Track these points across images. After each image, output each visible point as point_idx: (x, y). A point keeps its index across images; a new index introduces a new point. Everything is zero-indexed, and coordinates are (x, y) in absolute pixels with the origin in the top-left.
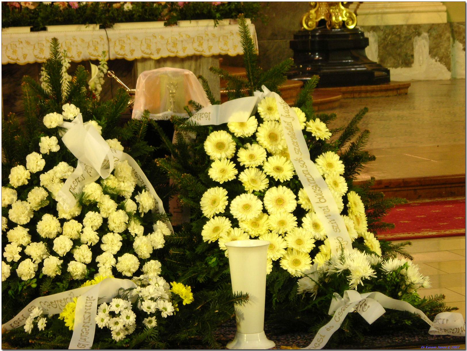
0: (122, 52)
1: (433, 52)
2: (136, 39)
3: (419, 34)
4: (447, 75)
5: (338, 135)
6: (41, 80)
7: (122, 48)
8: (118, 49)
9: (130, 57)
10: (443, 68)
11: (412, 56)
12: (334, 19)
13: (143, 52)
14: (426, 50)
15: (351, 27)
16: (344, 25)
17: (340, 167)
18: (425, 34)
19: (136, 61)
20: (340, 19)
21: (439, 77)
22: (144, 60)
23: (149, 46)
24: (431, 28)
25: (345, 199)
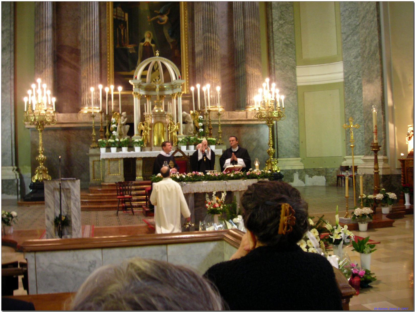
0: (230, 189)
1: (300, 178)
2: (234, 185)
3: (295, 172)
4: (304, 185)
5: (316, 223)
6: (206, 197)
7: (230, 188)
8: (229, 188)
9: (232, 190)
10: (302, 182)
11: (293, 179)
12: (273, 169)
13: (236, 189)
14: (298, 177)
15: (278, 172)
16: (276, 171)
17: (317, 233)
18: (297, 172)
19: (234, 191)
20: (275, 169)
21: (302, 185)
22: (236, 191)
23: (238, 187)
24: (299, 170)
25: (319, 242)
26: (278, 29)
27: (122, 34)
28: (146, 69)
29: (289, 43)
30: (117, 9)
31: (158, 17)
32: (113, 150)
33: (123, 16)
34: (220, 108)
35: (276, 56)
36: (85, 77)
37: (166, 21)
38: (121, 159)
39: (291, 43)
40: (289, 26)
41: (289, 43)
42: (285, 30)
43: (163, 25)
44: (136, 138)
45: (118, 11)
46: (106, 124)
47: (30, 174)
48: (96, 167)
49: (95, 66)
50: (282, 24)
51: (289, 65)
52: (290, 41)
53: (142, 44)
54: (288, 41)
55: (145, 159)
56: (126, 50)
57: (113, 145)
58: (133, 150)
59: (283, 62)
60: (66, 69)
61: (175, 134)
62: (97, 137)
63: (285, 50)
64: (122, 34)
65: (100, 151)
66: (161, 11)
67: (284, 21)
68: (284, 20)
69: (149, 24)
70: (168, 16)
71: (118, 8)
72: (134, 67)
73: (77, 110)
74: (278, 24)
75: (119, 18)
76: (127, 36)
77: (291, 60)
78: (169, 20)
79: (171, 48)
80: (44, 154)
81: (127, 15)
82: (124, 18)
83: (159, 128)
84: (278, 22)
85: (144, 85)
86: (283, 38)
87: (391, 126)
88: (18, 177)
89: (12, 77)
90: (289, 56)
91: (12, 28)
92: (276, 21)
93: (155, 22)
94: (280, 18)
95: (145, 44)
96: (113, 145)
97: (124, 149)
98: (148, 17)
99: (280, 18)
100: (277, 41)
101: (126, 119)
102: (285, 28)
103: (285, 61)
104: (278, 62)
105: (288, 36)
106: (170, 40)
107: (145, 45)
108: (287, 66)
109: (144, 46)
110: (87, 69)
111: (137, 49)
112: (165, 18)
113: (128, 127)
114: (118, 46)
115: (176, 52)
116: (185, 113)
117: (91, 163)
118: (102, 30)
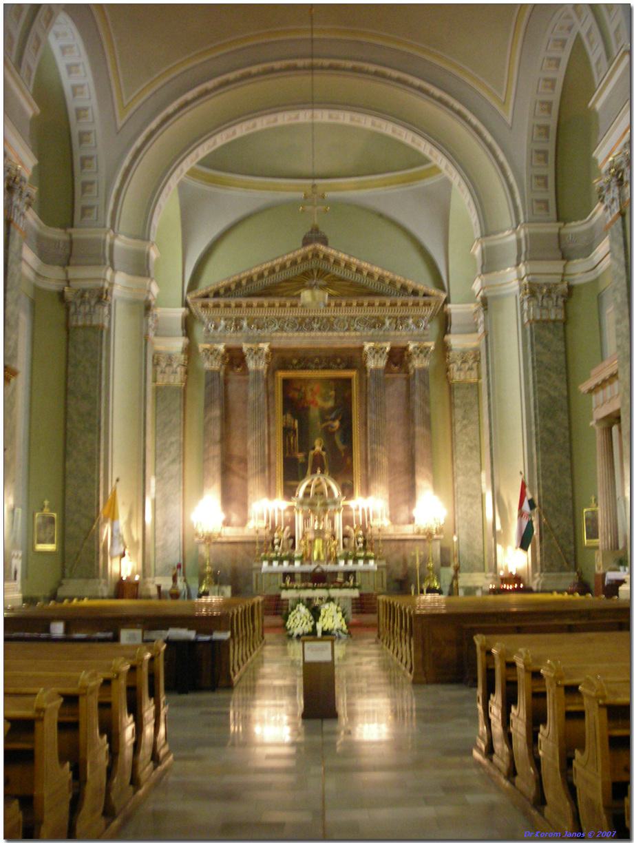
28: (309, 487)
31: (329, 423)
32: (275, 563)
34: (386, 522)
35: (458, 462)
37: (337, 427)
44: (297, 554)
46: (270, 538)
47: (197, 586)
48: (259, 580)
56: (296, 460)
57: (276, 559)
58: (294, 564)
59: (466, 466)
60: (235, 480)
61: (332, 549)
62: (261, 551)
63: (469, 453)
65: (262, 564)
66: (333, 416)
70: (340, 421)
72: (304, 476)
73: (244, 523)
76: (297, 446)
78: (341, 426)
79: (343, 455)
80: (210, 565)
83: (318, 543)
85: (308, 501)
87: (499, 547)
88: (185, 587)
89: (181, 488)
91: (182, 439)
94: (464, 418)
96: (276, 559)
97: (286, 563)
98: (319, 423)
99: (464, 418)
101: (289, 535)
102: (469, 428)
106: (341, 447)
109: (315, 456)
111: (306, 457)
112: (337, 424)
113: (291, 542)
114: (287, 455)
115: (348, 461)
116: (348, 527)
117: (254, 576)
118: (272, 438)
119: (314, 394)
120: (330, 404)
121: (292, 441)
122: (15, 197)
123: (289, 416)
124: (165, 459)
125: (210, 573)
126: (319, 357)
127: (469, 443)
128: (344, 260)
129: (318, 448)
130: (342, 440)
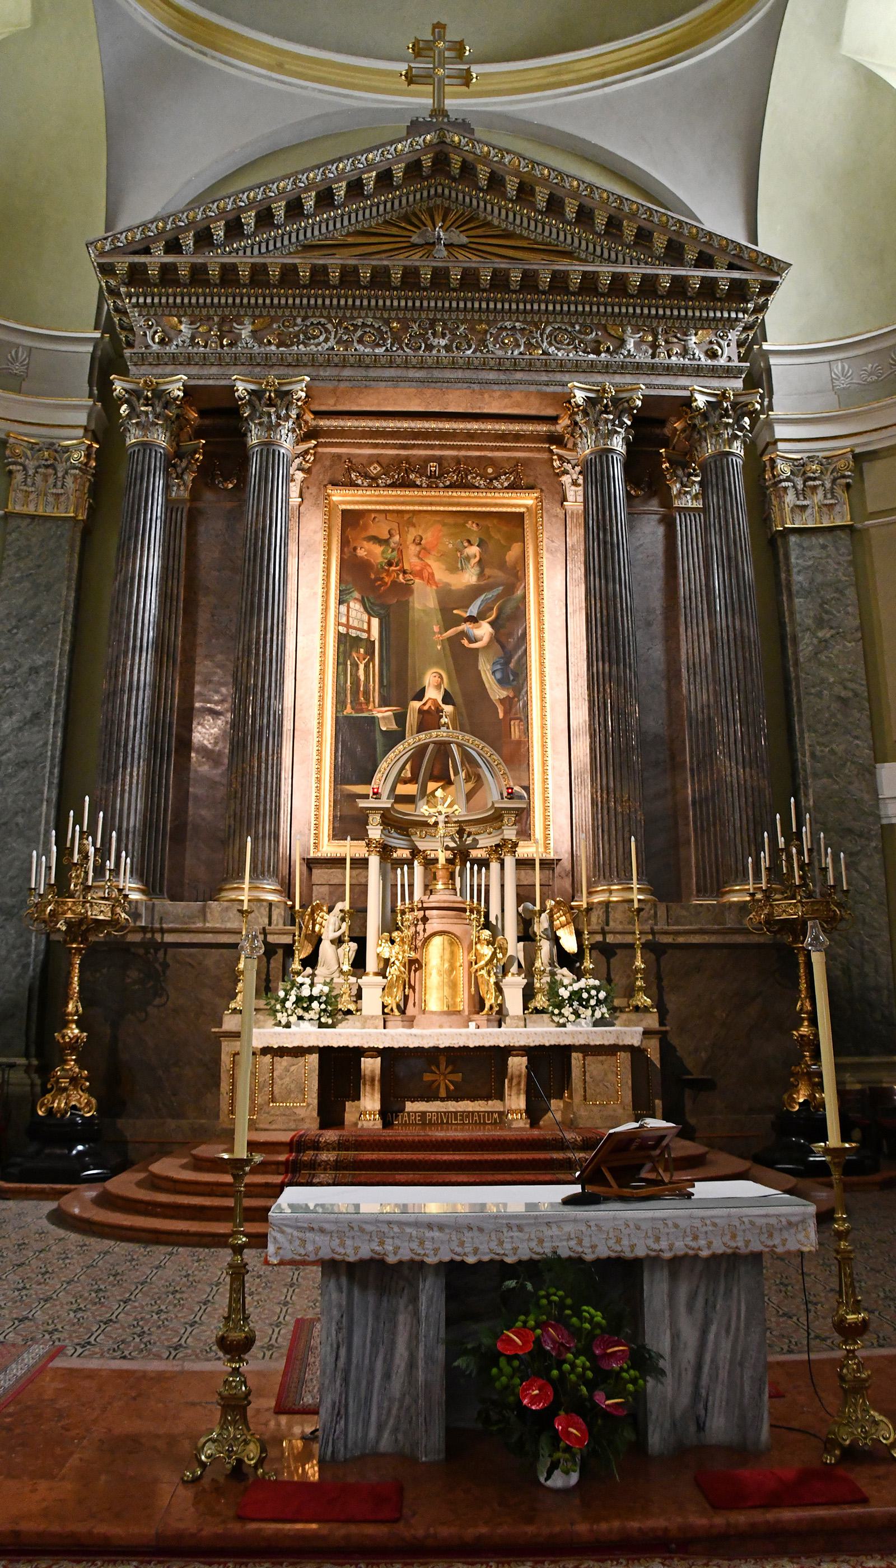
26: (816, 654)
27: (362, 678)
29: (850, 694)
30: (348, 607)
31: (465, 627)
33: (365, 627)
36: (236, 792)
37: (486, 639)
38: (310, 1050)
39: (856, 695)
40: (849, 645)
41: (850, 694)
42: (837, 656)
43: (477, 650)
45: (352, 613)
49: (267, 760)
50: (826, 641)
51: (853, 763)
52: (853, 690)
53: (416, 705)
54: (845, 688)
55: (389, 1055)
59: (833, 752)
63: (839, 716)
64: (362, 678)
66: (473, 610)
67: (833, 632)
68: (831, 628)
69: (439, 647)
71: (352, 604)
74: (815, 641)
75: (353, 633)
77: (857, 746)
81: (375, 622)
82: (369, 631)
84: (814, 634)
86: (831, 680)
90: (855, 734)
92: (808, 629)
93: (454, 643)
94: (820, 623)
95: (424, 704)
98: (436, 629)
100: (813, 691)
103: (840, 749)
104: (818, 753)
105: (846, 675)
107: (426, 708)
108: (849, 764)
109: (420, 711)
110: (243, 769)
111: (400, 718)
112: (484, 631)
119: (424, 551)
120: (470, 577)
121: (361, 673)
122: (29, 520)
123: (356, 606)
124: (11, 713)
125: (73, 1045)
126: (439, 460)
127: (838, 690)
128: (517, 174)
129: (433, 694)
130: (499, 675)
